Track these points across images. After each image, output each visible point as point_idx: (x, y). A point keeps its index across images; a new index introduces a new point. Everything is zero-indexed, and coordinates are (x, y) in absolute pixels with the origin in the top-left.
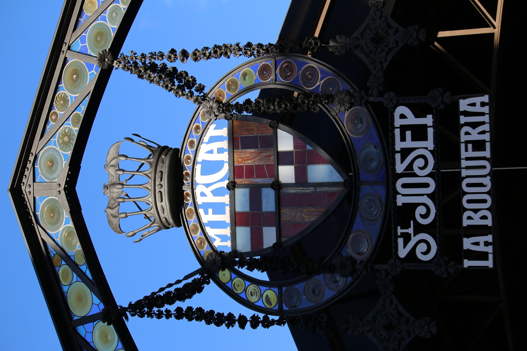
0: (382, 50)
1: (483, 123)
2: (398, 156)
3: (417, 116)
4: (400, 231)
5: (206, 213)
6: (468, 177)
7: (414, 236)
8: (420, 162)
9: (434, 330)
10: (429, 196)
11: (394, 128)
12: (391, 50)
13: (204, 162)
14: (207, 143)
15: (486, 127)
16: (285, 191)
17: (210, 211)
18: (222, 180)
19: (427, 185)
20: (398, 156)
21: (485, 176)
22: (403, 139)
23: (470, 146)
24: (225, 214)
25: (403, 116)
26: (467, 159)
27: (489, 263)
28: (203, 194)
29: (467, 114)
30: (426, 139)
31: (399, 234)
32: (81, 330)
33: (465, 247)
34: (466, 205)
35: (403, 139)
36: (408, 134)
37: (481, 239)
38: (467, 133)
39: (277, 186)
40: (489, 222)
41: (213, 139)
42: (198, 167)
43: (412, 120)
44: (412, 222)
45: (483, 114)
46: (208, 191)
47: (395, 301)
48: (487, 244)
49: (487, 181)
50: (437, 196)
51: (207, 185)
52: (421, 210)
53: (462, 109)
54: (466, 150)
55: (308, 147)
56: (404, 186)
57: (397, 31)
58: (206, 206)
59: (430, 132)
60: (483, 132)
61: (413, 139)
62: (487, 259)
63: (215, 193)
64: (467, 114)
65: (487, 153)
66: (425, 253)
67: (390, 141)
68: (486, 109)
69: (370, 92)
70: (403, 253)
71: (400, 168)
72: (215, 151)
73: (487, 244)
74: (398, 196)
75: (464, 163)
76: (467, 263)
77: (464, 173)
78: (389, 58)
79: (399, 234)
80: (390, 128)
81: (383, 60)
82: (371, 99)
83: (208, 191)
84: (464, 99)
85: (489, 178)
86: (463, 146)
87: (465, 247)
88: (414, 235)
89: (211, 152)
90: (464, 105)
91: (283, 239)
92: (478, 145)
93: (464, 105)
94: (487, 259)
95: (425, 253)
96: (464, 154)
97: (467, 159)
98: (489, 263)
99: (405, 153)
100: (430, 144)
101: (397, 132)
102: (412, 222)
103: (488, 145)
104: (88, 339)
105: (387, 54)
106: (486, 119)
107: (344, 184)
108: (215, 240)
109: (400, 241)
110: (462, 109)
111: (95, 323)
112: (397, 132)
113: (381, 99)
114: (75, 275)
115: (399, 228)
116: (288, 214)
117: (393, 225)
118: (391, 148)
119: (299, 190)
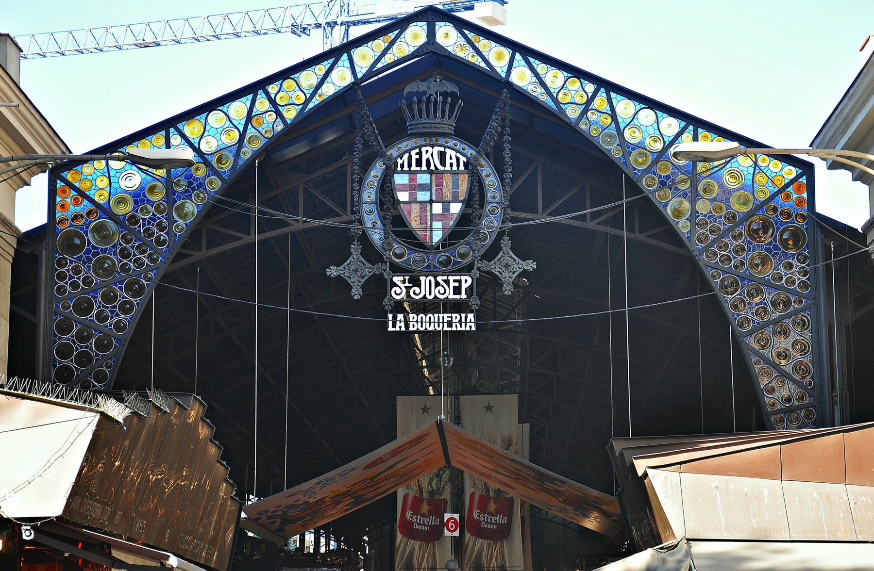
0: (502, 269)
1: (461, 327)
2: (445, 278)
3: (466, 289)
4: (407, 278)
5: (417, 154)
6: (434, 317)
7: (405, 286)
8: (442, 291)
9: (355, 297)
10: (425, 295)
11: (460, 276)
12: (501, 274)
13: (445, 153)
14: (456, 156)
15: (459, 329)
16: (428, 205)
17: (418, 157)
18: (435, 166)
19: (430, 294)
20: (445, 278)
21: (434, 327)
22: (455, 281)
23: (450, 319)
24: (416, 167)
25: (466, 281)
26: (443, 317)
27: (390, 329)
28: (427, 151)
29: (466, 318)
30: (454, 294)
31: (405, 277)
32: (345, 57)
33: (398, 315)
34: (420, 316)
35: (455, 281)
36: (457, 284)
37: (403, 324)
38: (456, 317)
39: (431, 202)
40: (411, 329)
41: (458, 159)
42: (442, 149)
43: (464, 286)
44: (411, 285)
45: (466, 327)
46: (429, 155)
47: (370, 274)
48: (400, 327)
49: (431, 328)
50: (425, 300)
51: (432, 155)
52: (417, 290)
53: (469, 315)
54: (447, 317)
55: (452, 222)
56: (430, 281)
57: (511, 277)
58: (420, 154)
59: (457, 297)
60: (456, 327)
61: (454, 287)
62: (393, 327)
63: (428, 160)
64: (466, 318)
65: (446, 328)
66: (395, 291)
67: (454, 274)
68: (468, 329)
69: (480, 262)
70: (397, 279)
71: (440, 279)
72: (451, 161)
73: (400, 327)
74: (425, 277)
75: (441, 315)
76: (390, 316)
77: (436, 315)
78: (497, 273)
79: (405, 277)
80: (460, 274)
81: (496, 270)
82: (476, 263)
83: (429, 155)
84: (474, 316)
85: (434, 329)
86: (450, 315)
87: (398, 315)
88: (405, 286)
89: (451, 158)
90: (471, 316)
91: (401, 205)
92: (450, 324)
93: (471, 316)
94: (393, 327)
95: (395, 291)
96: (446, 315)
97: (443, 317)
98: (390, 329)
99: (447, 282)
100: (452, 296)
101: (458, 278)
102: (411, 285)
103: (450, 329)
104: (340, 63)
105: (499, 272)
106: (463, 329)
107: (432, 246)
108: (401, 159)
109: (402, 278)
110: (468, 314)
111: (350, 69)
112: (458, 278)
113: (476, 268)
114: (379, 54)
115: (409, 277)
116: (415, 207)
117: (410, 274)
118: (450, 274)
119: (428, 218)
